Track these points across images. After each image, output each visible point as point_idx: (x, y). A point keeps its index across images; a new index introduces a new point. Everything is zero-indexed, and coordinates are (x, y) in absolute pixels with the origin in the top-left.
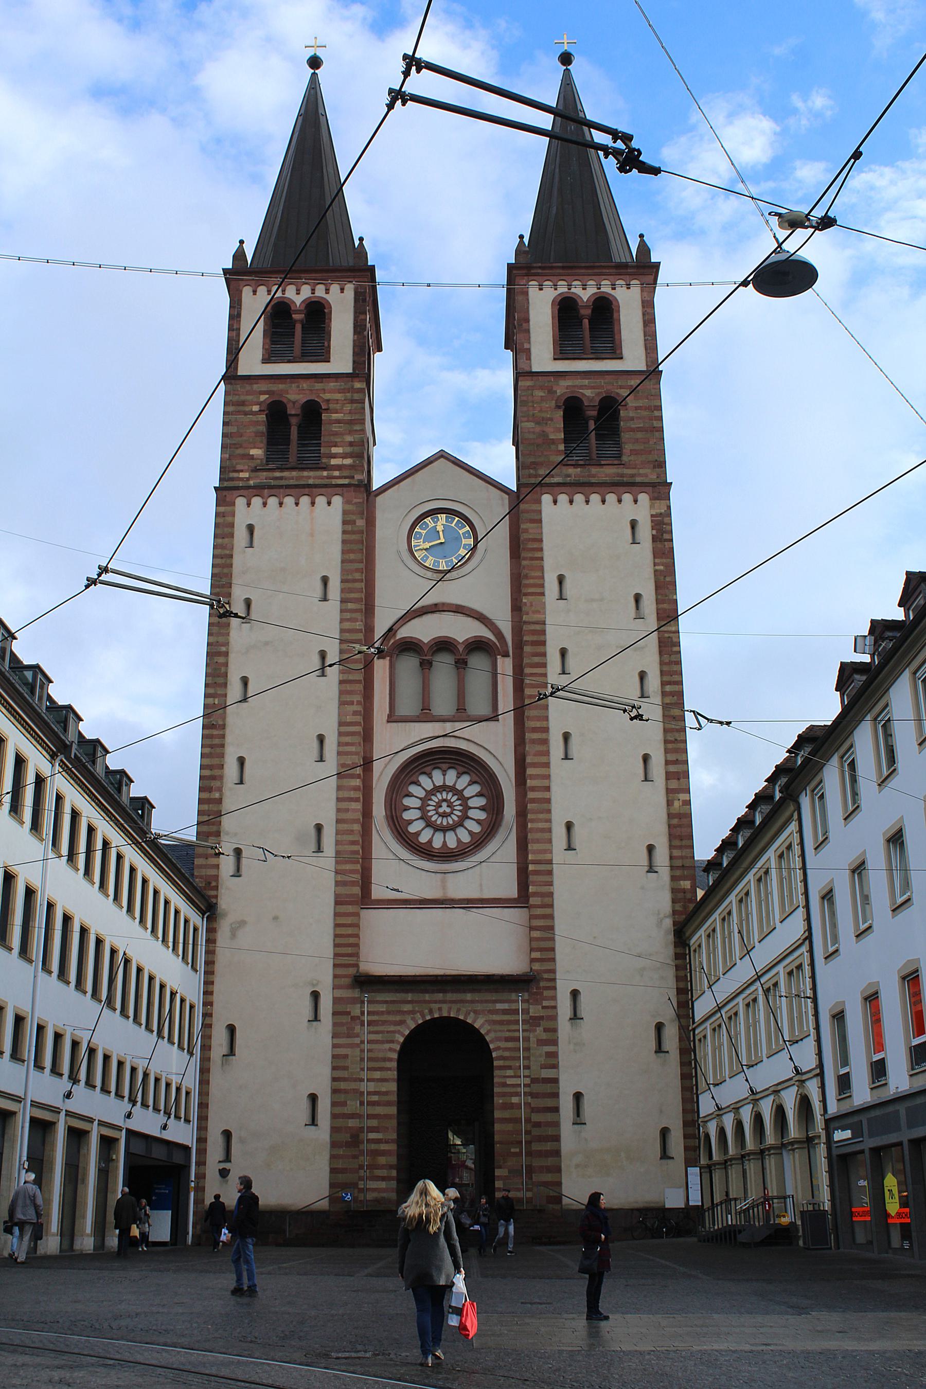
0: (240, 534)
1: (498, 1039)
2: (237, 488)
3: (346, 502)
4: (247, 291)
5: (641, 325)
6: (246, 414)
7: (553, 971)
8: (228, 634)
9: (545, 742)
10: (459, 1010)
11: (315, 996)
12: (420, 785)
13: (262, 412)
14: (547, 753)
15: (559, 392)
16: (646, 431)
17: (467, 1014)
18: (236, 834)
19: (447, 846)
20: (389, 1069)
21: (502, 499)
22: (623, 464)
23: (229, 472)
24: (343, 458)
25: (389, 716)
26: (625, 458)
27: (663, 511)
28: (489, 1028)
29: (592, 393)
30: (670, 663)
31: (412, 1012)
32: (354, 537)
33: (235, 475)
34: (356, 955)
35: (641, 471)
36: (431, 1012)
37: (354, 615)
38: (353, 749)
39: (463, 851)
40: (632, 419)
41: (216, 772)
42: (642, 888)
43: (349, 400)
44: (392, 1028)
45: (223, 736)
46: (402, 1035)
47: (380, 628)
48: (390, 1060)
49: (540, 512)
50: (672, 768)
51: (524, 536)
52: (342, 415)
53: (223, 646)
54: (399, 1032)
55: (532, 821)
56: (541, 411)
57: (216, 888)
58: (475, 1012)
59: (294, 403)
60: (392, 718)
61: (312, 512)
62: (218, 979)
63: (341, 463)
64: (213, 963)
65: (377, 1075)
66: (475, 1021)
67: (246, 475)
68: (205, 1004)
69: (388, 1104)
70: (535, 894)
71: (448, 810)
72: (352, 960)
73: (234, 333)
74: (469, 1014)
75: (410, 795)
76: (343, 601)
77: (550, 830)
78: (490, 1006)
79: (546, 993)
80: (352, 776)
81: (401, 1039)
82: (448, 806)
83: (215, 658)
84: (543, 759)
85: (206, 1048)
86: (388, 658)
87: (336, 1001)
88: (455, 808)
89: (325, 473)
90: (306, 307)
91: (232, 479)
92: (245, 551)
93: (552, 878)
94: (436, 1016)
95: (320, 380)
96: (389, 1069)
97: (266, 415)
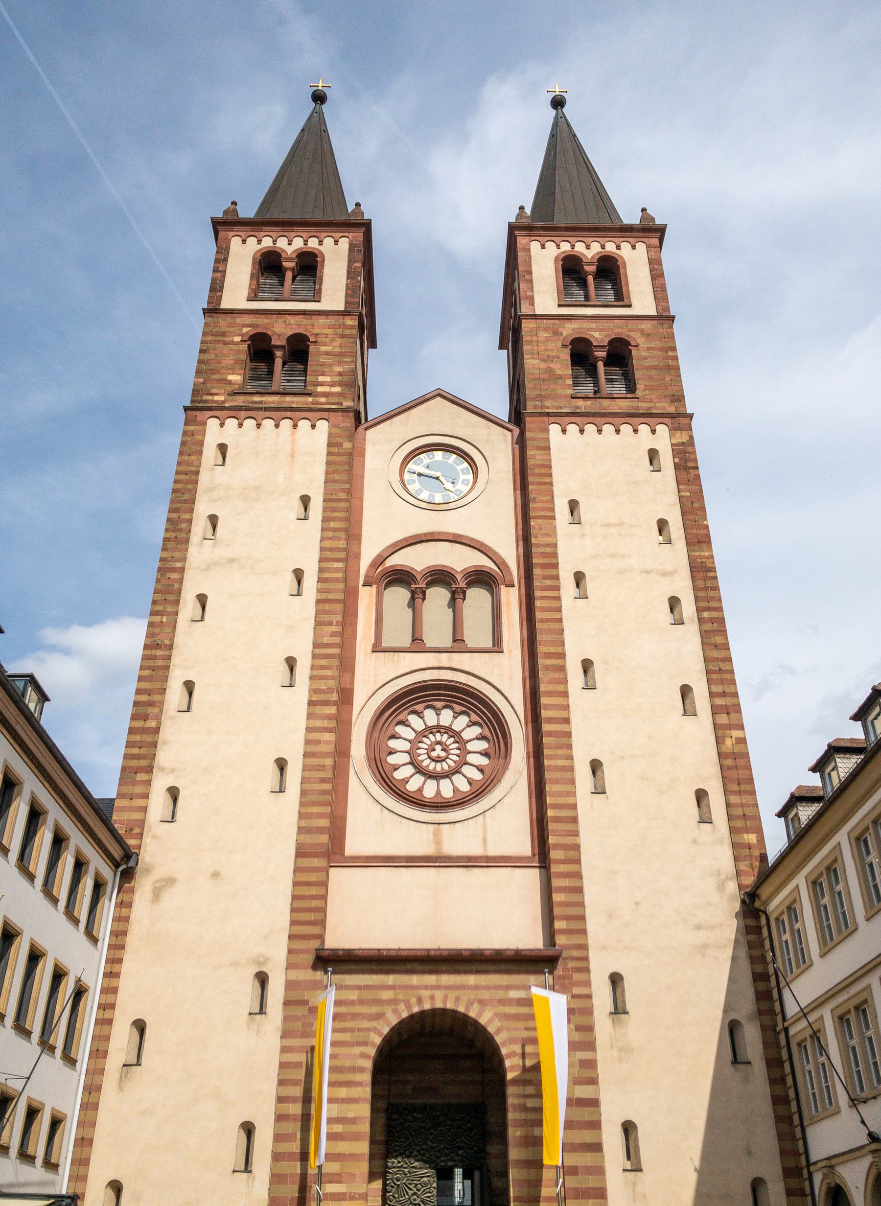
0: (210, 452)
1: (512, 1041)
2: (210, 409)
3: (332, 426)
4: (235, 243)
5: (649, 279)
6: (226, 343)
7: (584, 947)
8: (187, 550)
9: (562, 669)
10: (457, 999)
11: (262, 979)
12: (409, 726)
13: (244, 343)
14: (565, 681)
15: (565, 333)
16: (662, 369)
17: (470, 1004)
18: (173, 770)
19: (441, 795)
20: (360, 1084)
21: (505, 435)
22: (638, 398)
23: (203, 394)
24: (331, 386)
25: (374, 646)
26: (639, 393)
27: (685, 440)
28: (500, 1024)
29: (600, 335)
30: (706, 588)
31: (394, 1002)
32: (338, 459)
33: (210, 398)
34: (322, 923)
35: (658, 405)
36: (420, 1001)
37: (337, 534)
38: (329, 673)
39: (463, 800)
40: (645, 358)
41: (157, 698)
42: (695, 842)
43: (340, 334)
44: (366, 1024)
45: (169, 658)
46: (379, 1033)
47: (368, 553)
48: (361, 1070)
49: (548, 440)
50: (719, 701)
51: (530, 462)
52: (332, 347)
53: (178, 561)
54: (375, 1030)
55: (551, 757)
56: (546, 350)
57: (140, 836)
58: (481, 1002)
59: (279, 335)
60: (377, 648)
61: (293, 434)
62: (128, 956)
63: (329, 391)
64: (124, 933)
65: (342, 1092)
66: (480, 1014)
67: (222, 398)
68: (105, 991)
69: (355, 1137)
70: (557, 846)
71: (443, 754)
72: (315, 930)
73: (219, 275)
74: (472, 1004)
75: (396, 736)
76: (325, 520)
77: (571, 769)
78: (501, 994)
79: (577, 977)
80: (326, 703)
81: (378, 1040)
82: (442, 750)
83: (168, 574)
84: (560, 688)
85: (99, 1053)
86: (376, 586)
87: (290, 985)
88: (451, 752)
89: (310, 399)
90: (297, 257)
91: (206, 401)
92: (213, 469)
93: (577, 827)
94: (427, 1006)
95: (309, 317)
96: (360, 1084)
97: (249, 346)
